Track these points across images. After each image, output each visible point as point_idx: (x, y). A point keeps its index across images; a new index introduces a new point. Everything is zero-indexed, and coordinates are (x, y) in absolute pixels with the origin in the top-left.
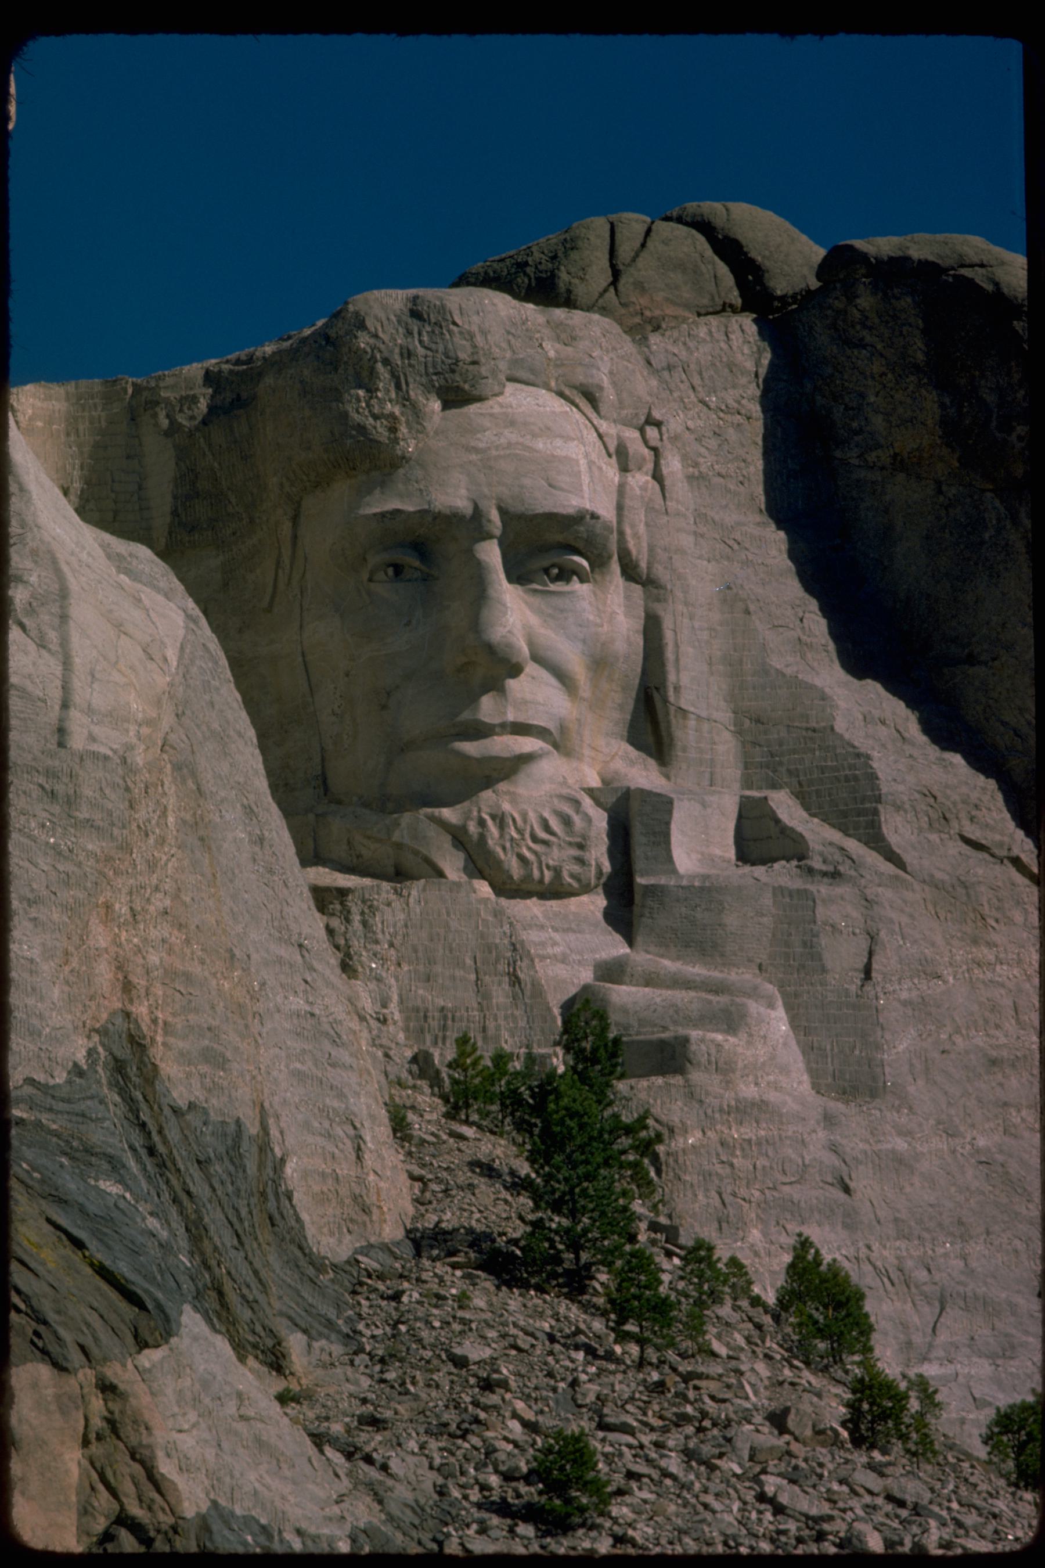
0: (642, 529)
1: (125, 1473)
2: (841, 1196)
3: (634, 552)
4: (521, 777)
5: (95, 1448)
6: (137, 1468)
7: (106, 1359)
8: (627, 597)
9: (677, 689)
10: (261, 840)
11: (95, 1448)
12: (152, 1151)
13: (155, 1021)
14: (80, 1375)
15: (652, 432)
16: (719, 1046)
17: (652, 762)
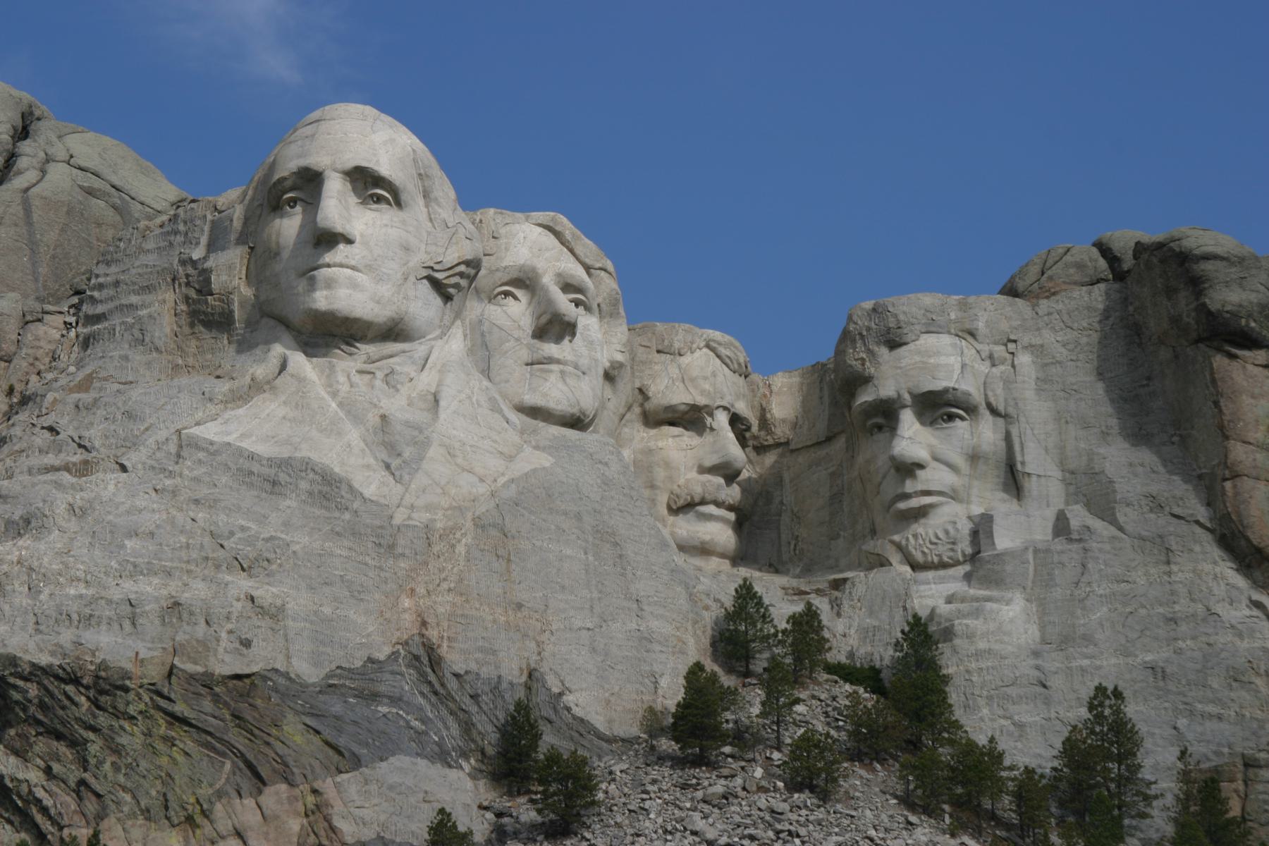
0: (999, 391)
1: (321, 826)
2: (1043, 690)
3: (994, 404)
4: (931, 515)
5: (312, 818)
6: (326, 824)
7: (316, 779)
8: (994, 424)
9: (1023, 463)
10: (621, 556)
11: (312, 818)
12: (436, 693)
13: (442, 637)
14: (301, 787)
15: (1011, 346)
16: (967, 626)
17: (1015, 501)
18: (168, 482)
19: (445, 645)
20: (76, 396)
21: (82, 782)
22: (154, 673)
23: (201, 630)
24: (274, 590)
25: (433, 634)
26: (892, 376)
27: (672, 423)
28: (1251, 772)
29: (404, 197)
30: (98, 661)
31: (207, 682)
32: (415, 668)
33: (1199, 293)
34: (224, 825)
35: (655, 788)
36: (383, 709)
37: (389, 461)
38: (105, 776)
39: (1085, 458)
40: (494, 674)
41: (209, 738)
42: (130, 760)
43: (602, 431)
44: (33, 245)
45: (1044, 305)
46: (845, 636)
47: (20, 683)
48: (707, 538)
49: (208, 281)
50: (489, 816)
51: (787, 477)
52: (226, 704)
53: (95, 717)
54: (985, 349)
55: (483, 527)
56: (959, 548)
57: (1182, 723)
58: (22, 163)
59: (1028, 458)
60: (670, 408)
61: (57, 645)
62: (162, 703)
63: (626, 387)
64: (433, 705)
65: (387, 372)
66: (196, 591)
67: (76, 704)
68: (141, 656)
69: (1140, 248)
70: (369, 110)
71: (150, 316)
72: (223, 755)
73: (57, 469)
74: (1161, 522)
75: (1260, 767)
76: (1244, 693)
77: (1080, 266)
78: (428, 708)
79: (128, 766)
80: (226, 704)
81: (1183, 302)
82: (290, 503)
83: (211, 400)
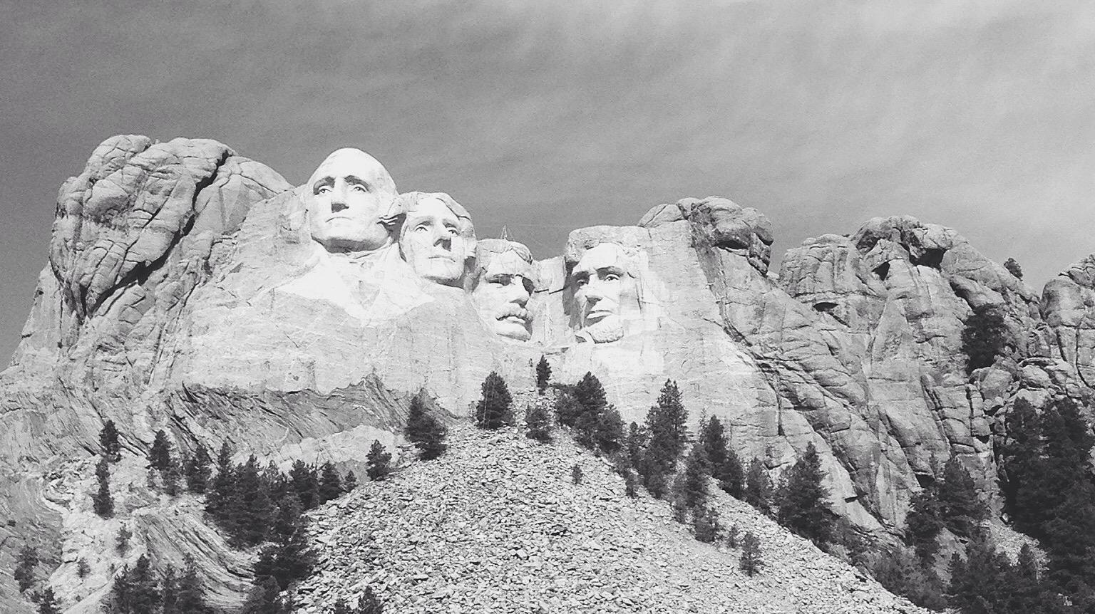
19: (384, 377)
20: (232, 274)
21: (228, 437)
22: (257, 391)
23: (278, 373)
24: (308, 356)
25: (378, 374)
26: (587, 262)
28: (734, 427)
29: (370, 188)
30: (234, 386)
31: (279, 395)
32: (371, 388)
33: (714, 226)
34: (286, 455)
35: (470, 438)
36: (357, 406)
37: (361, 300)
38: (237, 436)
39: (668, 296)
40: (405, 391)
41: (280, 418)
42: (247, 428)
43: (465, 286)
44: (222, 210)
45: (653, 230)
46: (566, 372)
47: (202, 396)
48: (512, 331)
49: (289, 225)
50: (400, 450)
51: (548, 304)
52: (287, 404)
53: (232, 410)
54: (627, 250)
55: (401, 328)
56: (614, 334)
57: (706, 407)
58: (220, 175)
60: (496, 276)
61: (219, 380)
62: (261, 404)
64: (378, 403)
65: (362, 263)
66: (276, 356)
67: (225, 405)
68: (252, 384)
69: (693, 207)
71: (265, 239)
72: (286, 426)
73: (222, 305)
75: (737, 425)
78: (376, 405)
79: (246, 430)
80: (287, 404)
81: (709, 230)
82: (319, 318)
83: (288, 275)
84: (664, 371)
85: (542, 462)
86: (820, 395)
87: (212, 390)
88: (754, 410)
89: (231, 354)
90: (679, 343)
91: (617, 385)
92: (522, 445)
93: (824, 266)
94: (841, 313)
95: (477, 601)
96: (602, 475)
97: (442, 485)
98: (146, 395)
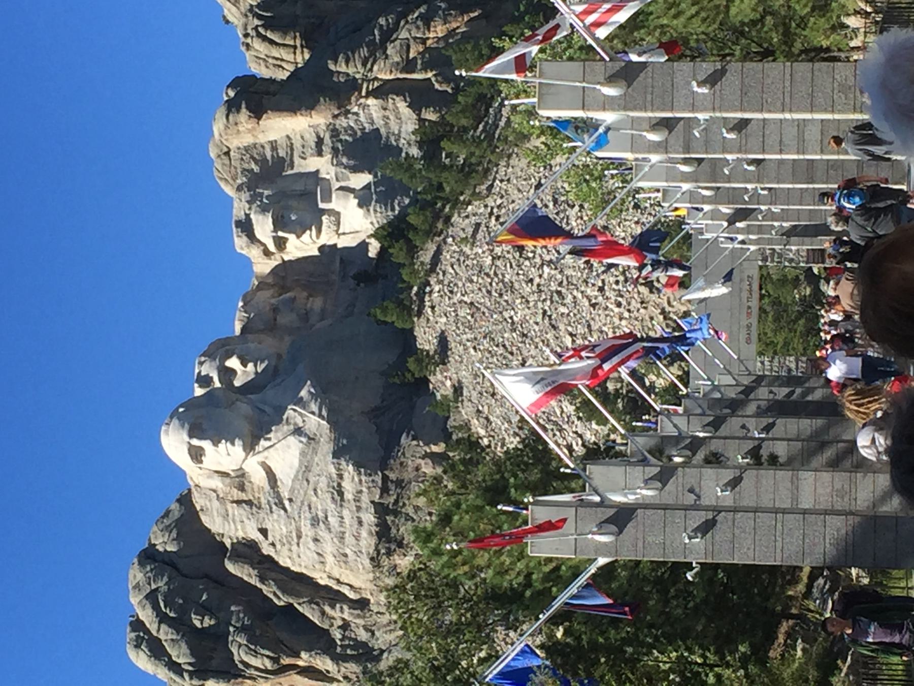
18: (306, 503)
27: (275, 320)
31: (385, 490)
59: (298, 188)
63: (262, 336)
70: (163, 428)
74: (325, 142)
76: (391, 117)
77: (224, 164)
84: (370, 173)
85: (452, 272)
86: (397, 42)
87: (377, 546)
88: (408, 99)
89: (344, 533)
90: (344, 160)
91: (379, 215)
92: (437, 288)
93: (269, 34)
94: (313, 23)
95: (576, 311)
96: (467, 221)
97: (472, 351)
98: (375, 608)
